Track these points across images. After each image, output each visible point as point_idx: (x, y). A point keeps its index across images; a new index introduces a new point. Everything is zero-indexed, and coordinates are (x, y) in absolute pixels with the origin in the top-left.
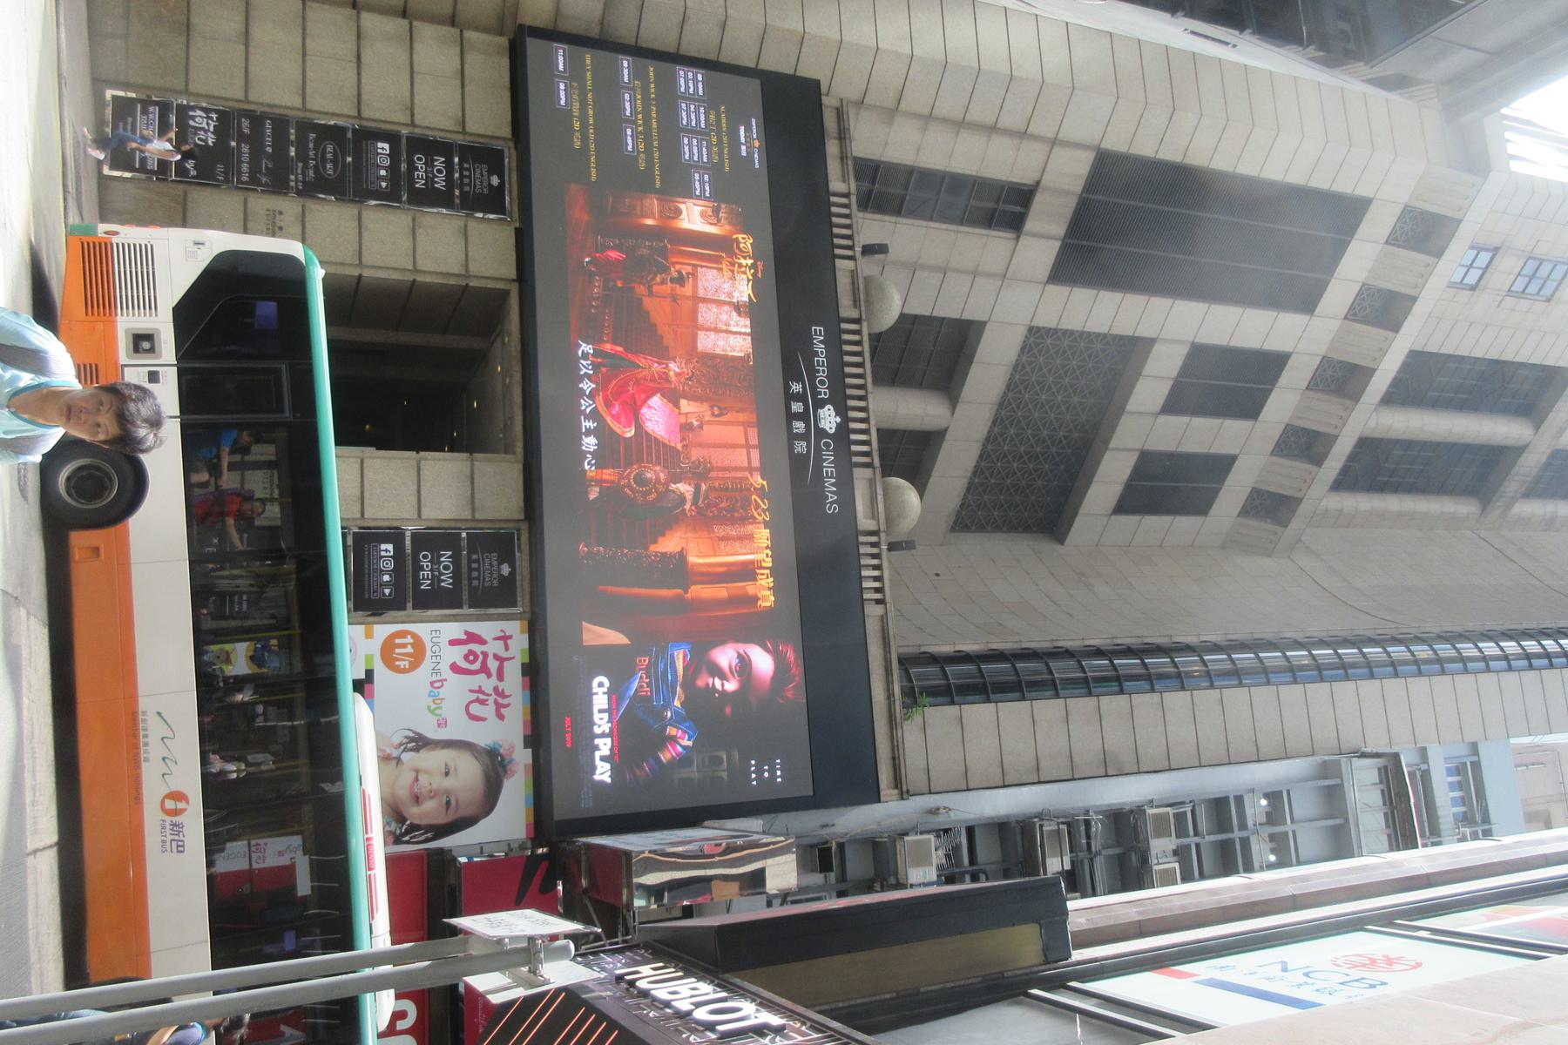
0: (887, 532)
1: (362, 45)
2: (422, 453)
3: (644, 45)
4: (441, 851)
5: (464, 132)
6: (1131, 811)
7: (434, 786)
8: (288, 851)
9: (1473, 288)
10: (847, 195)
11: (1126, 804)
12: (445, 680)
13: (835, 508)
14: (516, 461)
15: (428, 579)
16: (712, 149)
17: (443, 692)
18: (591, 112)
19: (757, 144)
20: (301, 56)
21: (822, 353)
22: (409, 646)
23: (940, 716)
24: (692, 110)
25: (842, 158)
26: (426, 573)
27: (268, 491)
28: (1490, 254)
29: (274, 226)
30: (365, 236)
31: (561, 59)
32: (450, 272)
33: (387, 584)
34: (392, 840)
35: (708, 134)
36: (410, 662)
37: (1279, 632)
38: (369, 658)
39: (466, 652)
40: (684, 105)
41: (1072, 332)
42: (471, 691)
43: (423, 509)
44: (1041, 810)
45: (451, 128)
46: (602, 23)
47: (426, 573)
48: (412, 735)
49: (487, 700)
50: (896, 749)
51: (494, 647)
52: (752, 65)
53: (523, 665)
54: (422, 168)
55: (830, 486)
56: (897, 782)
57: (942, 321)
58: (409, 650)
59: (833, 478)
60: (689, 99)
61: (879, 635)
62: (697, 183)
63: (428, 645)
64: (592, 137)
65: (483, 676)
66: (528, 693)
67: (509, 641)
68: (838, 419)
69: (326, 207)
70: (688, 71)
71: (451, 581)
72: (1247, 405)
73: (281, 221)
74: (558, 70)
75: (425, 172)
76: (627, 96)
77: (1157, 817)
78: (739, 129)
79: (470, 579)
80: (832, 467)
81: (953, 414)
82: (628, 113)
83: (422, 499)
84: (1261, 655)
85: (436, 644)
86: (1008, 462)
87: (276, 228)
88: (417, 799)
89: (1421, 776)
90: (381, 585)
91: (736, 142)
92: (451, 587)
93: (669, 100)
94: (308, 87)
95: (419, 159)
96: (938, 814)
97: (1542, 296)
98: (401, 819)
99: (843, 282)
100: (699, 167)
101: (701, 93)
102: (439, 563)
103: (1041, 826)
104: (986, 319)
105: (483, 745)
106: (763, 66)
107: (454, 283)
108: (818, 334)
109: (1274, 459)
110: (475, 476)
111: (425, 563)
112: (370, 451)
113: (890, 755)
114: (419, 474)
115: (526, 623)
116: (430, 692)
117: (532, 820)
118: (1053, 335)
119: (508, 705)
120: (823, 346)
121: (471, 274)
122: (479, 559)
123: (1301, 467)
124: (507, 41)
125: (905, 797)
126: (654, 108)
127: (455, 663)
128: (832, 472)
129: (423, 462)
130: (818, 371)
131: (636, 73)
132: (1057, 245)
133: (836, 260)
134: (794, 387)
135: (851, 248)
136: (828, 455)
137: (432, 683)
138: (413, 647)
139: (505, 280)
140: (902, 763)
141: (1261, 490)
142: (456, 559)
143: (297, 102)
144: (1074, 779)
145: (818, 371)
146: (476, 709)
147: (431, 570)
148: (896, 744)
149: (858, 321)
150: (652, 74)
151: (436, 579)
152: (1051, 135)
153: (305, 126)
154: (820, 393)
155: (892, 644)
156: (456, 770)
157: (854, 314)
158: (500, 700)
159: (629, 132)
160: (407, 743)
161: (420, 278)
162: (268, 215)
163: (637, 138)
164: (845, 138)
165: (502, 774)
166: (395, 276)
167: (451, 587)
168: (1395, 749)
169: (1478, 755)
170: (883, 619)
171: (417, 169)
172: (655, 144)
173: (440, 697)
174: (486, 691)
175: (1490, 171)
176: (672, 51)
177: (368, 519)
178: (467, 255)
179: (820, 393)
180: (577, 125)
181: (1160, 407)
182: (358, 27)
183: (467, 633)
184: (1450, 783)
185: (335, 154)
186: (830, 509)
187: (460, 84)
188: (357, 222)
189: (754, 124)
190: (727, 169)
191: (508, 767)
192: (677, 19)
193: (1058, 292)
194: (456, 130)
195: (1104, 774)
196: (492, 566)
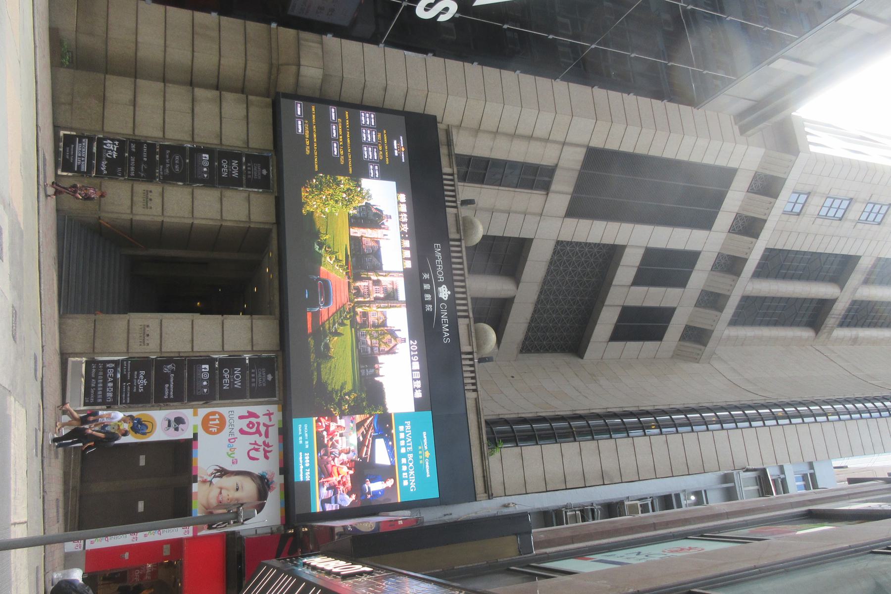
0: (477, 353)
2: (225, 316)
3: (344, 101)
4: (233, 533)
5: (248, 147)
6: (617, 503)
7: (231, 496)
9: (798, 214)
10: (452, 175)
11: (614, 499)
12: (237, 438)
13: (448, 340)
14: (275, 319)
15: (227, 383)
17: (235, 445)
18: (315, 136)
19: (403, 149)
20: (163, 111)
21: (440, 257)
22: (217, 420)
23: (509, 453)
25: (449, 156)
28: (806, 196)
29: (147, 198)
30: (196, 203)
31: (299, 109)
32: (241, 220)
33: (205, 387)
34: (207, 527)
37: (699, 403)
38: (195, 427)
39: (248, 422)
40: (364, 131)
41: (581, 243)
42: (250, 444)
43: (225, 346)
44: (566, 504)
46: (321, 90)
47: (226, 380)
48: (219, 468)
49: (259, 449)
51: (263, 420)
52: (401, 109)
53: (279, 428)
54: (226, 166)
57: (510, 239)
58: (217, 422)
59: (447, 324)
60: (367, 127)
61: (474, 409)
62: (372, 171)
63: (227, 419)
64: (316, 148)
67: (271, 416)
68: (449, 293)
69: (175, 188)
71: (240, 384)
72: (681, 281)
73: (151, 196)
74: (298, 115)
75: (228, 168)
76: (334, 127)
77: (631, 506)
79: (251, 383)
80: (446, 318)
81: (517, 289)
82: (335, 135)
84: (688, 416)
85: (231, 418)
86: (550, 314)
87: (148, 200)
89: (781, 482)
90: (202, 387)
93: (356, 128)
94: (166, 126)
95: (224, 162)
96: (509, 507)
97: (837, 217)
99: (451, 220)
100: (373, 162)
101: (373, 124)
103: (566, 512)
104: (532, 237)
106: (407, 109)
107: (242, 226)
109: (697, 309)
112: (197, 315)
113: (482, 475)
114: (223, 327)
115: (281, 406)
118: (561, 244)
119: (270, 451)
122: (255, 372)
123: (711, 313)
125: (491, 498)
126: (349, 133)
127: (241, 429)
128: (446, 321)
129: (225, 320)
131: (340, 115)
132: (569, 197)
133: (447, 208)
134: (425, 276)
135: (455, 202)
136: (443, 312)
137: (229, 440)
138: (219, 420)
139: (270, 223)
140: (489, 480)
141: (691, 326)
143: (160, 135)
144: (585, 487)
146: (253, 454)
148: (485, 469)
149: (460, 240)
151: (232, 383)
152: (562, 140)
153: (164, 148)
155: (482, 413)
156: (242, 487)
157: (457, 236)
158: (266, 448)
159: (335, 145)
160: (215, 473)
161: (224, 224)
162: (144, 193)
164: (450, 145)
165: (268, 489)
166: (211, 223)
168: (764, 467)
169: (814, 469)
170: (477, 400)
171: (223, 167)
172: (349, 151)
174: (259, 444)
175: (799, 152)
176: (358, 103)
178: (249, 211)
180: (308, 143)
181: (631, 282)
182: (193, 95)
183: (248, 412)
184: (798, 486)
185: (180, 161)
186: (445, 341)
187: (246, 123)
189: (401, 139)
190: (387, 163)
191: (271, 485)
192: (362, 86)
193: (571, 222)
195: (602, 484)
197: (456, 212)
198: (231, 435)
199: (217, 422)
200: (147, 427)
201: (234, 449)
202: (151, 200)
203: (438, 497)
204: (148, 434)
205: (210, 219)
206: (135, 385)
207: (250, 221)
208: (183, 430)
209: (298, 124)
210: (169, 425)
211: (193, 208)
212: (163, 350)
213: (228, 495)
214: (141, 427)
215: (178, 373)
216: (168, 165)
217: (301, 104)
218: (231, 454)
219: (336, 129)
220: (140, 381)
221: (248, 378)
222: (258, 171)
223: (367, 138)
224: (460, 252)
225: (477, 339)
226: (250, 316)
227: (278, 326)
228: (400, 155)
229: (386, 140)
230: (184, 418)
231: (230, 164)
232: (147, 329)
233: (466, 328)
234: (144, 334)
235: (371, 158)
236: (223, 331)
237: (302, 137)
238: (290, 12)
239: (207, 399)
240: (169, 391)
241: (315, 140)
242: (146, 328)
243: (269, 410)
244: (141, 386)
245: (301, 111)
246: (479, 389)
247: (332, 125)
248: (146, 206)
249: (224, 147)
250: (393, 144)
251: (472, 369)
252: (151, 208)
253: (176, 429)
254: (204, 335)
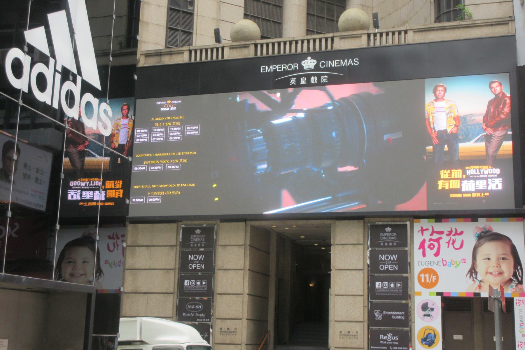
1: (140, 292)
2: (332, 268)
5: (176, 246)
7: (495, 265)
8: (522, 332)
12: (442, 259)
13: (356, 60)
14: (335, 223)
15: (393, 266)
16: (174, 125)
17: (449, 260)
18: (162, 186)
19: (169, 102)
21: (274, 67)
22: (425, 276)
24: (155, 135)
25: (171, 54)
26: (390, 267)
27: (351, 337)
31: (137, 200)
35: (168, 126)
36: (433, 275)
38: (431, 294)
39: (429, 249)
42: (448, 247)
43: (359, 268)
45: (175, 251)
48: (469, 275)
49: (453, 240)
50: (487, 24)
51: (427, 235)
53: (436, 221)
54: (195, 266)
55: (344, 63)
56: (504, 22)
58: (427, 275)
62: (192, 133)
63: (425, 267)
64: (174, 185)
65: (441, 241)
66: (450, 219)
67: (424, 228)
69: (217, 309)
70: (136, 137)
74: (143, 202)
76: (152, 168)
78: (162, 111)
79: (393, 246)
82: (160, 168)
83: (353, 268)
87: (228, 331)
88: (501, 273)
91: (169, 113)
92: (397, 255)
95: (191, 266)
98: (510, 281)
100: (184, 131)
101: (146, 131)
102: (385, 261)
105: (476, 241)
107: (249, 251)
108: (266, 69)
110: (343, 243)
111: (385, 267)
115: (415, 220)
116: (448, 266)
117: (515, 218)
119: (456, 229)
120: (271, 66)
121: (244, 244)
124: (130, 225)
125: (513, 19)
126: (157, 154)
128: (337, 62)
130: (284, 69)
134: (293, 82)
135: (217, 49)
137: (444, 265)
138: (426, 274)
142: (383, 253)
145: (284, 69)
146: (457, 245)
147: (388, 264)
148: (484, 24)
149: (256, 45)
150: (140, 156)
151: (393, 262)
154: (296, 68)
155: (429, 26)
156: (487, 255)
157: (252, 47)
158: (453, 233)
159: (169, 167)
161: (247, 267)
163: (172, 163)
164: (160, 53)
165: (490, 233)
166: (247, 279)
167: (397, 255)
170: (416, 31)
171: (195, 268)
172: (174, 154)
173: (451, 262)
177: (364, 293)
179: (296, 68)
180: (169, 193)
182: (131, 293)
183: (419, 249)
186: (356, 63)
188: (223, 295)
190: (183, 117)
191: (487, 230)
194: (175, 249)
196: (387, 236)
197: (228, 48)
198: (440, 264)
199: (427, 275)
200: (430, 334)
201: (452, 261)
202: (228, 329)
203: (508, 74)
204: (435, 333)
205: (244, 280)
206: (392, 343)
207: (244, 245)
208: (433, 305)
209: (152, 202)
210: (429, 315)
211: (234, 294)
212: (362, 320)
213: (493, 267)
214: (429, 339)
215: (383, 308)
216: (197, 315)
217: (132, 198)
218: (456, 263)
219: (154, 166)
220: (389, 339)
221: (385, 249)
222: (198, 237)
223: (161, 137)
224: (268, 45)
225: (354, 29)
226: (332, 246)
227: (340, 221)
228: (176, 105)
229: (161, 119)
230: (422, 304)
231: (192, 262)
232: (343, 333)
233: (343, 40)
234: (348, 335)
235: (179, 134)
236: (345, 270)
237: (164, 197)
238: (43, 209)
239: (405, 282)
240: (399, 315)
241: (166, 186)
242: (342, 334)
243: (419, 230)
244: (393, 338)
245: (139, 198)
246: (404, 28)
247: (151, 170)
248: (234, 333)
249: (177, 267)
250: (164, 111)
251: (384, 35)
252: (236, 329)
253: (432, 309)
254: (349, 285)
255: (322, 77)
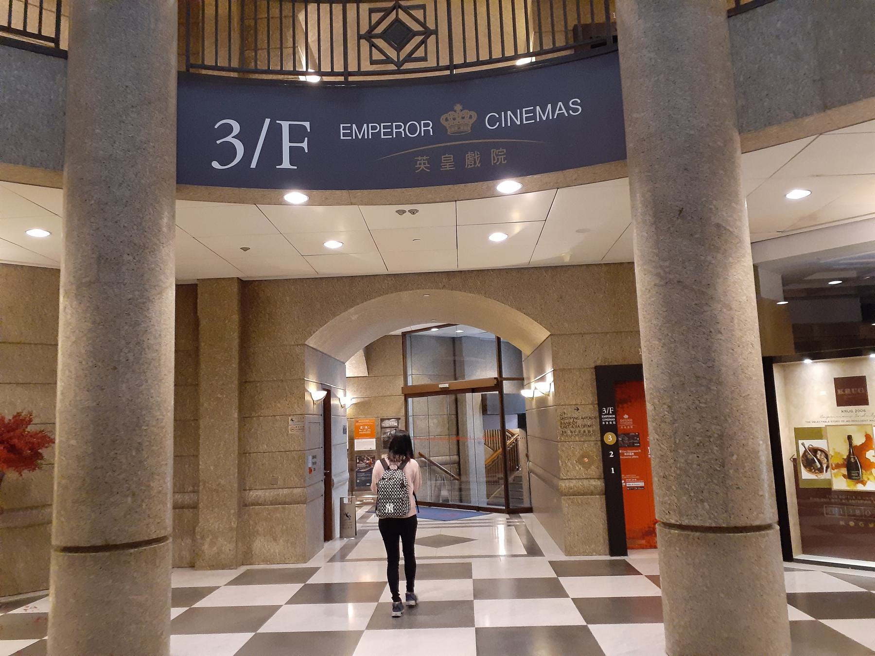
59: (535, 109)
68: (458, 107)
134: (422, 166)
255: (494, 151)
